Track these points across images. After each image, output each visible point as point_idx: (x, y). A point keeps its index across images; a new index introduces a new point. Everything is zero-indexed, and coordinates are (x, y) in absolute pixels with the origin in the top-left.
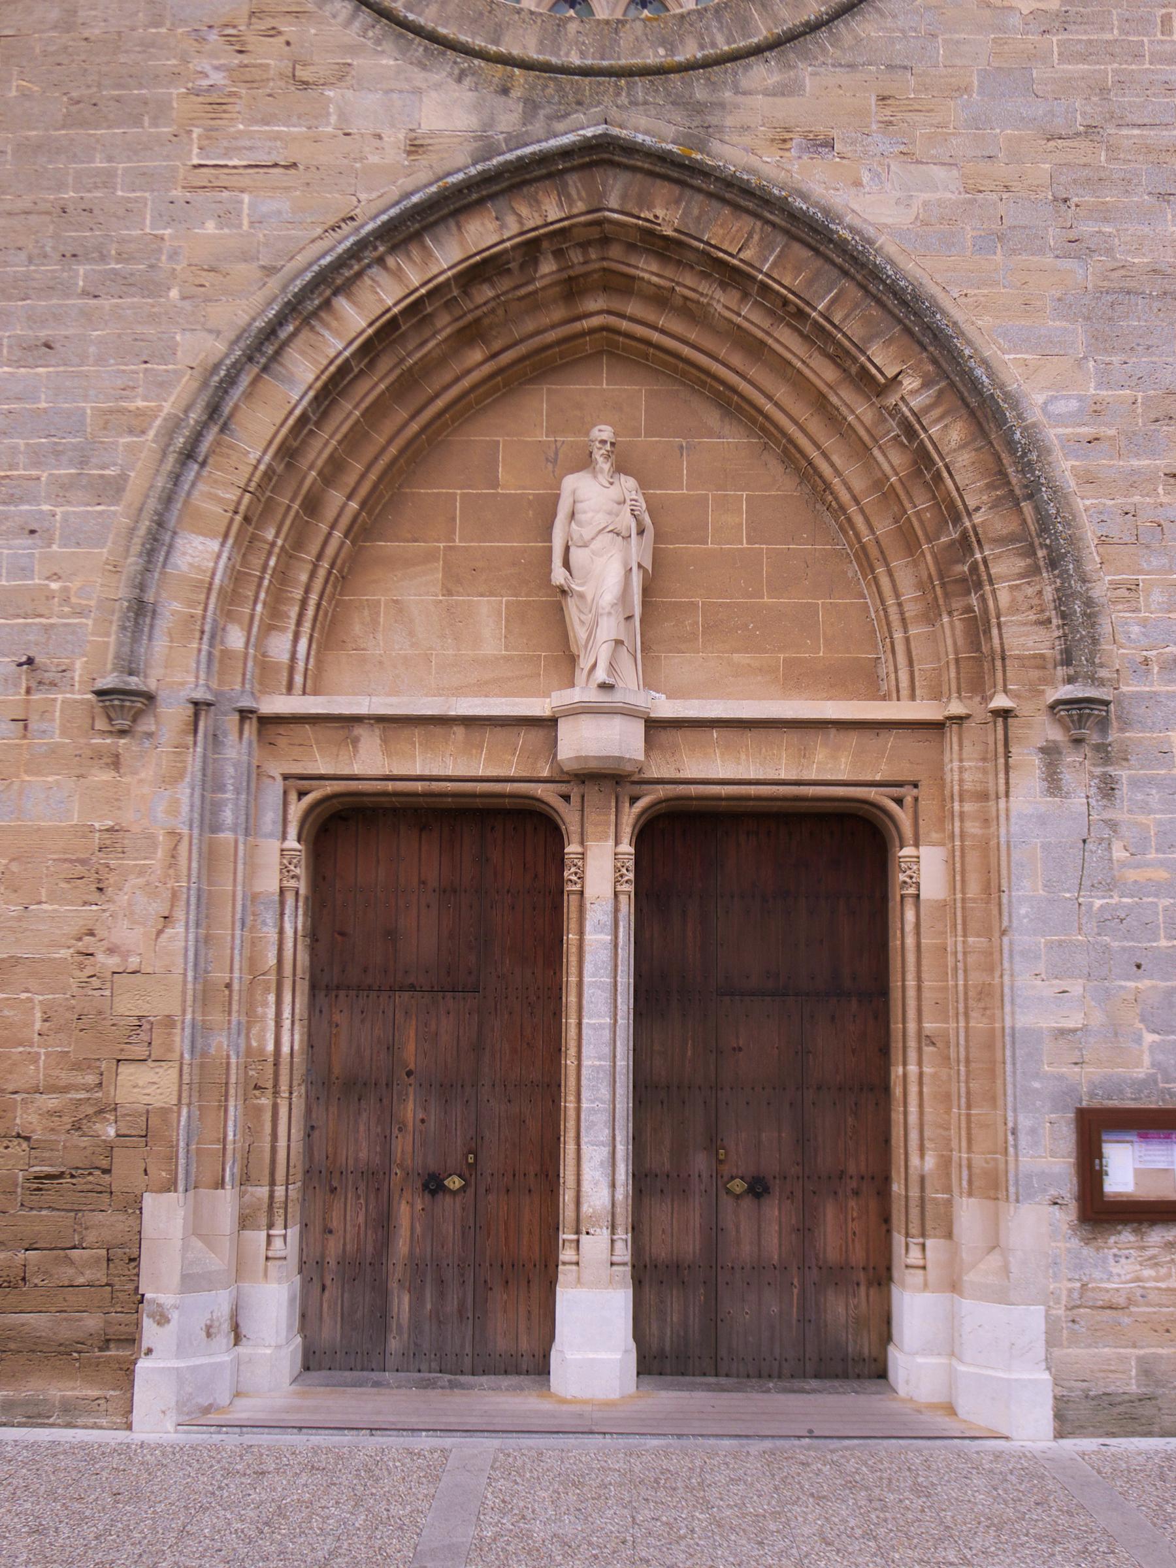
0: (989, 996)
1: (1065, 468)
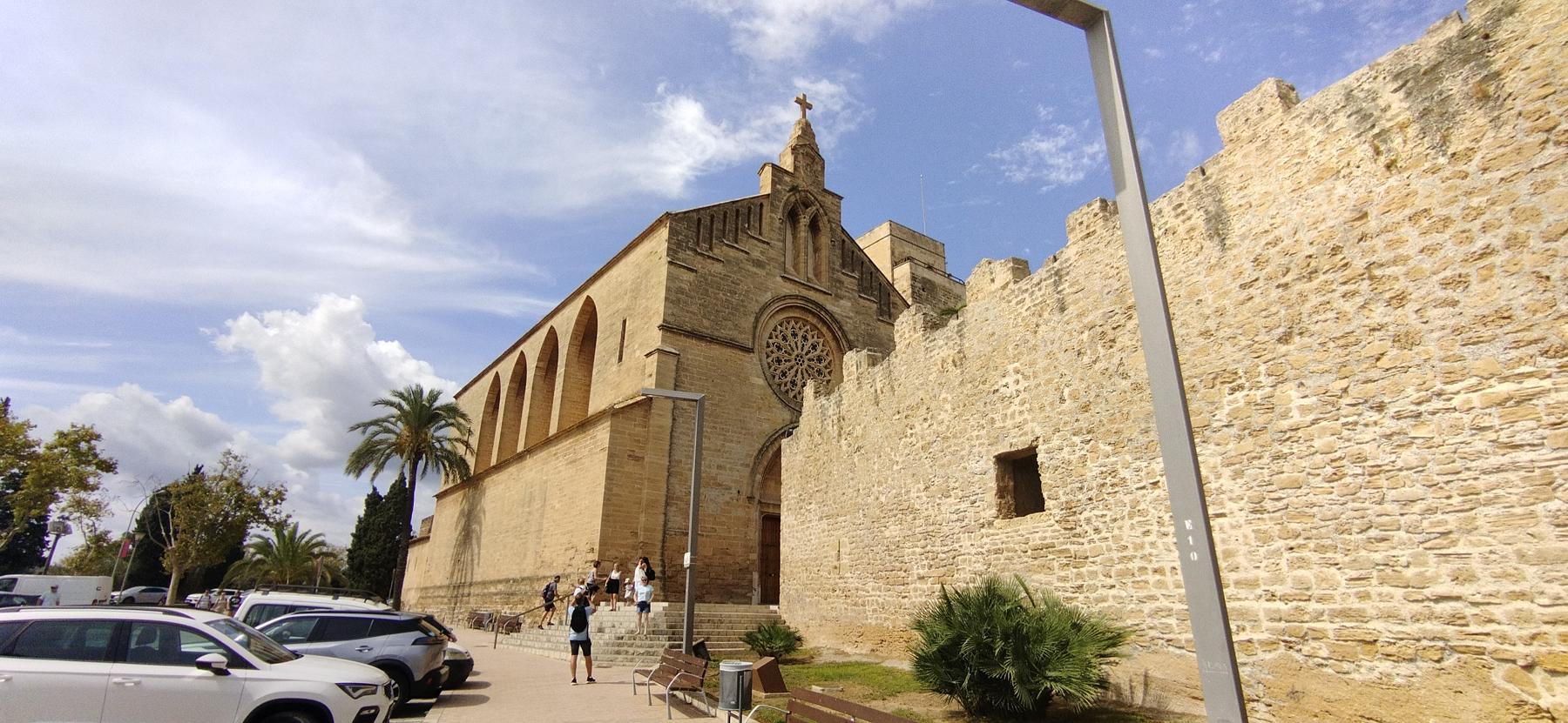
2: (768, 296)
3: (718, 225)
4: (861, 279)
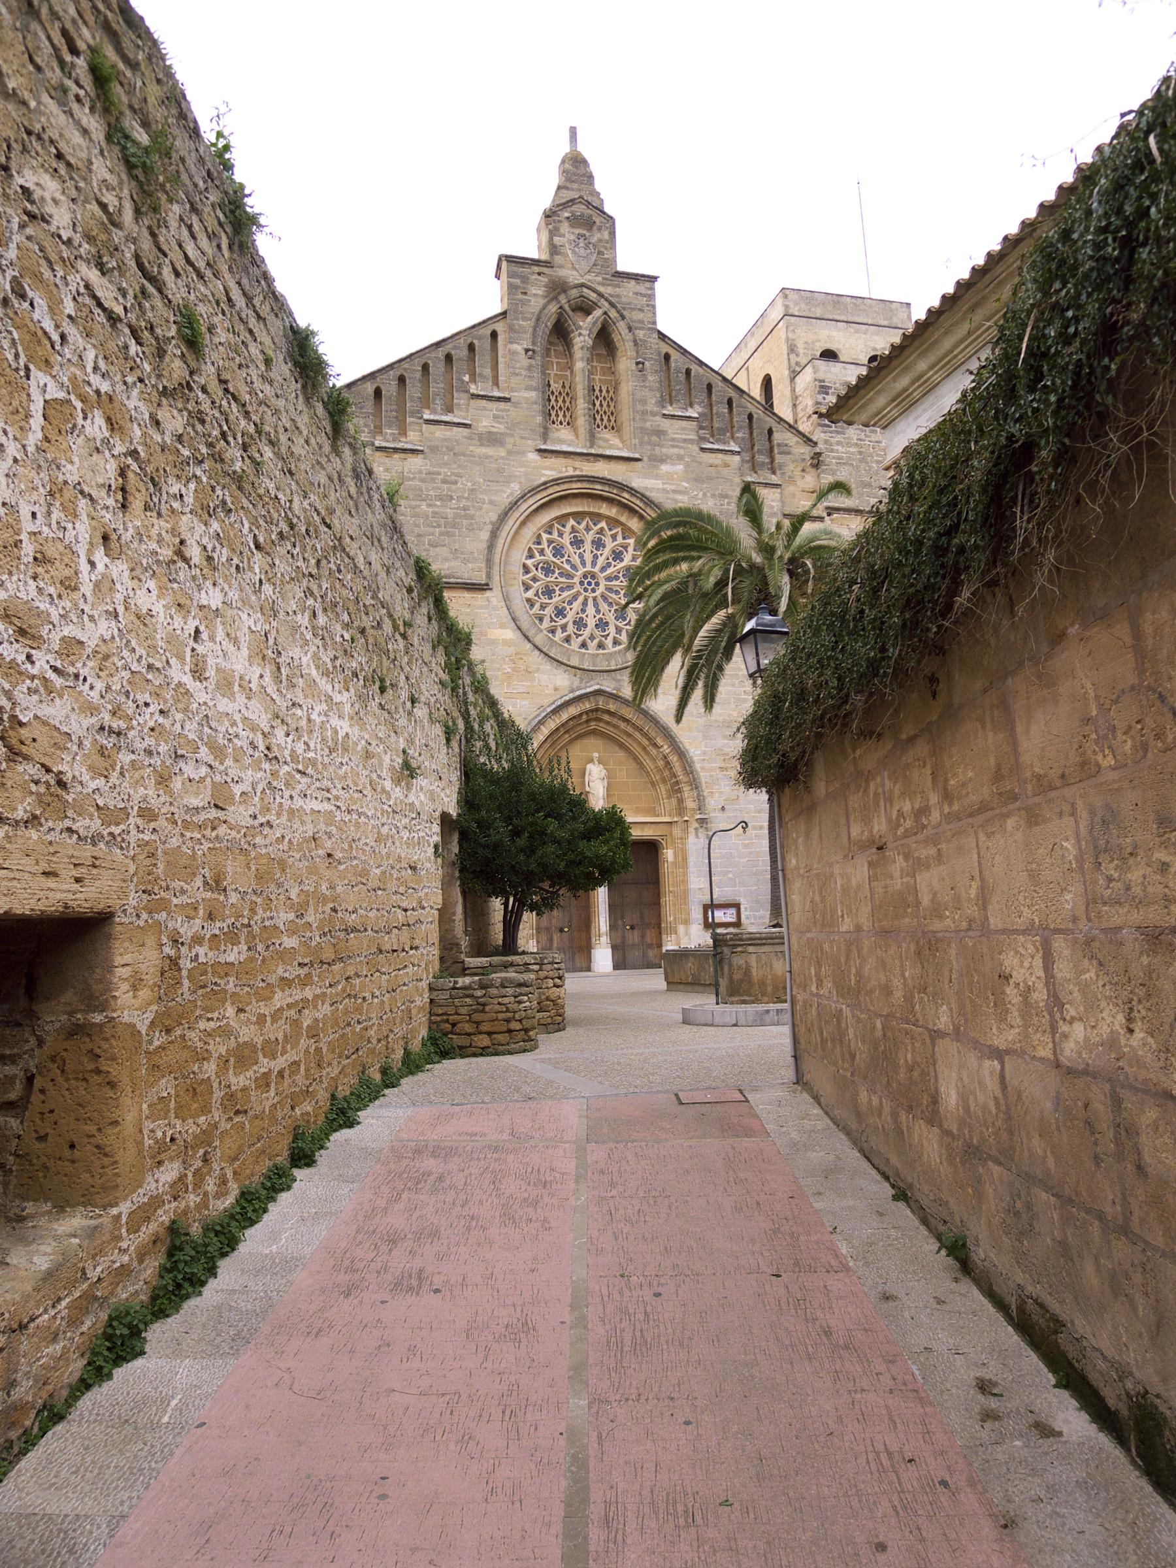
0: (685, 882)
1: (698, 766)
2: (516, 489)
3: (413, 390)
4: (709, 415)
